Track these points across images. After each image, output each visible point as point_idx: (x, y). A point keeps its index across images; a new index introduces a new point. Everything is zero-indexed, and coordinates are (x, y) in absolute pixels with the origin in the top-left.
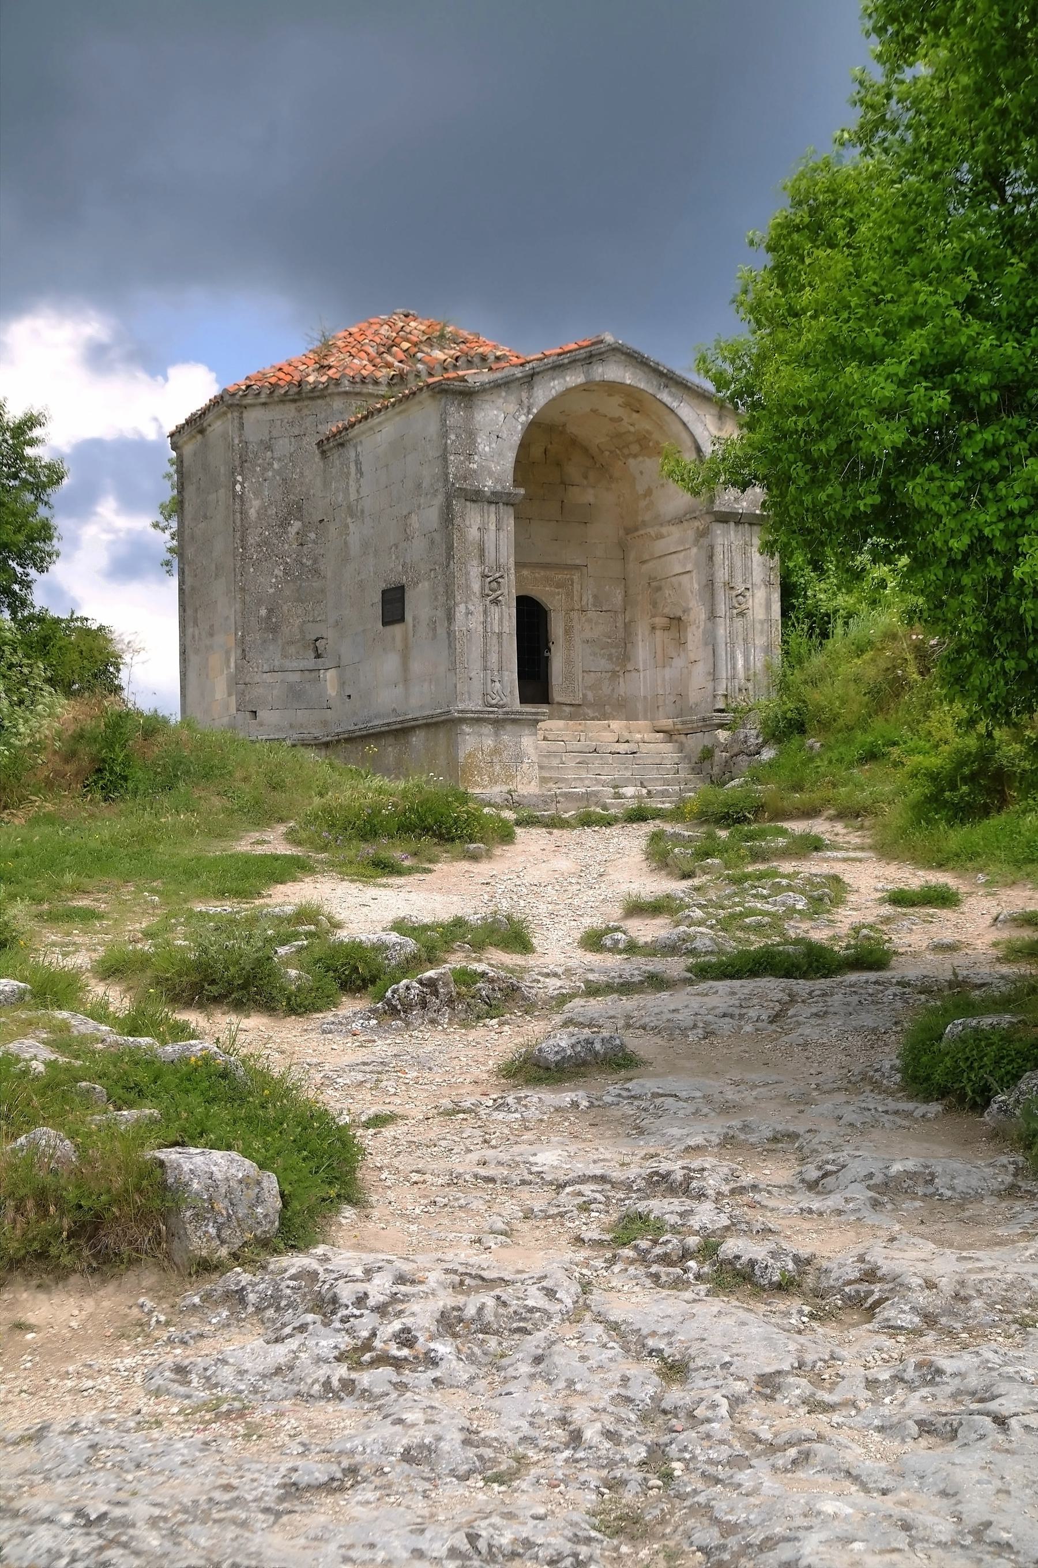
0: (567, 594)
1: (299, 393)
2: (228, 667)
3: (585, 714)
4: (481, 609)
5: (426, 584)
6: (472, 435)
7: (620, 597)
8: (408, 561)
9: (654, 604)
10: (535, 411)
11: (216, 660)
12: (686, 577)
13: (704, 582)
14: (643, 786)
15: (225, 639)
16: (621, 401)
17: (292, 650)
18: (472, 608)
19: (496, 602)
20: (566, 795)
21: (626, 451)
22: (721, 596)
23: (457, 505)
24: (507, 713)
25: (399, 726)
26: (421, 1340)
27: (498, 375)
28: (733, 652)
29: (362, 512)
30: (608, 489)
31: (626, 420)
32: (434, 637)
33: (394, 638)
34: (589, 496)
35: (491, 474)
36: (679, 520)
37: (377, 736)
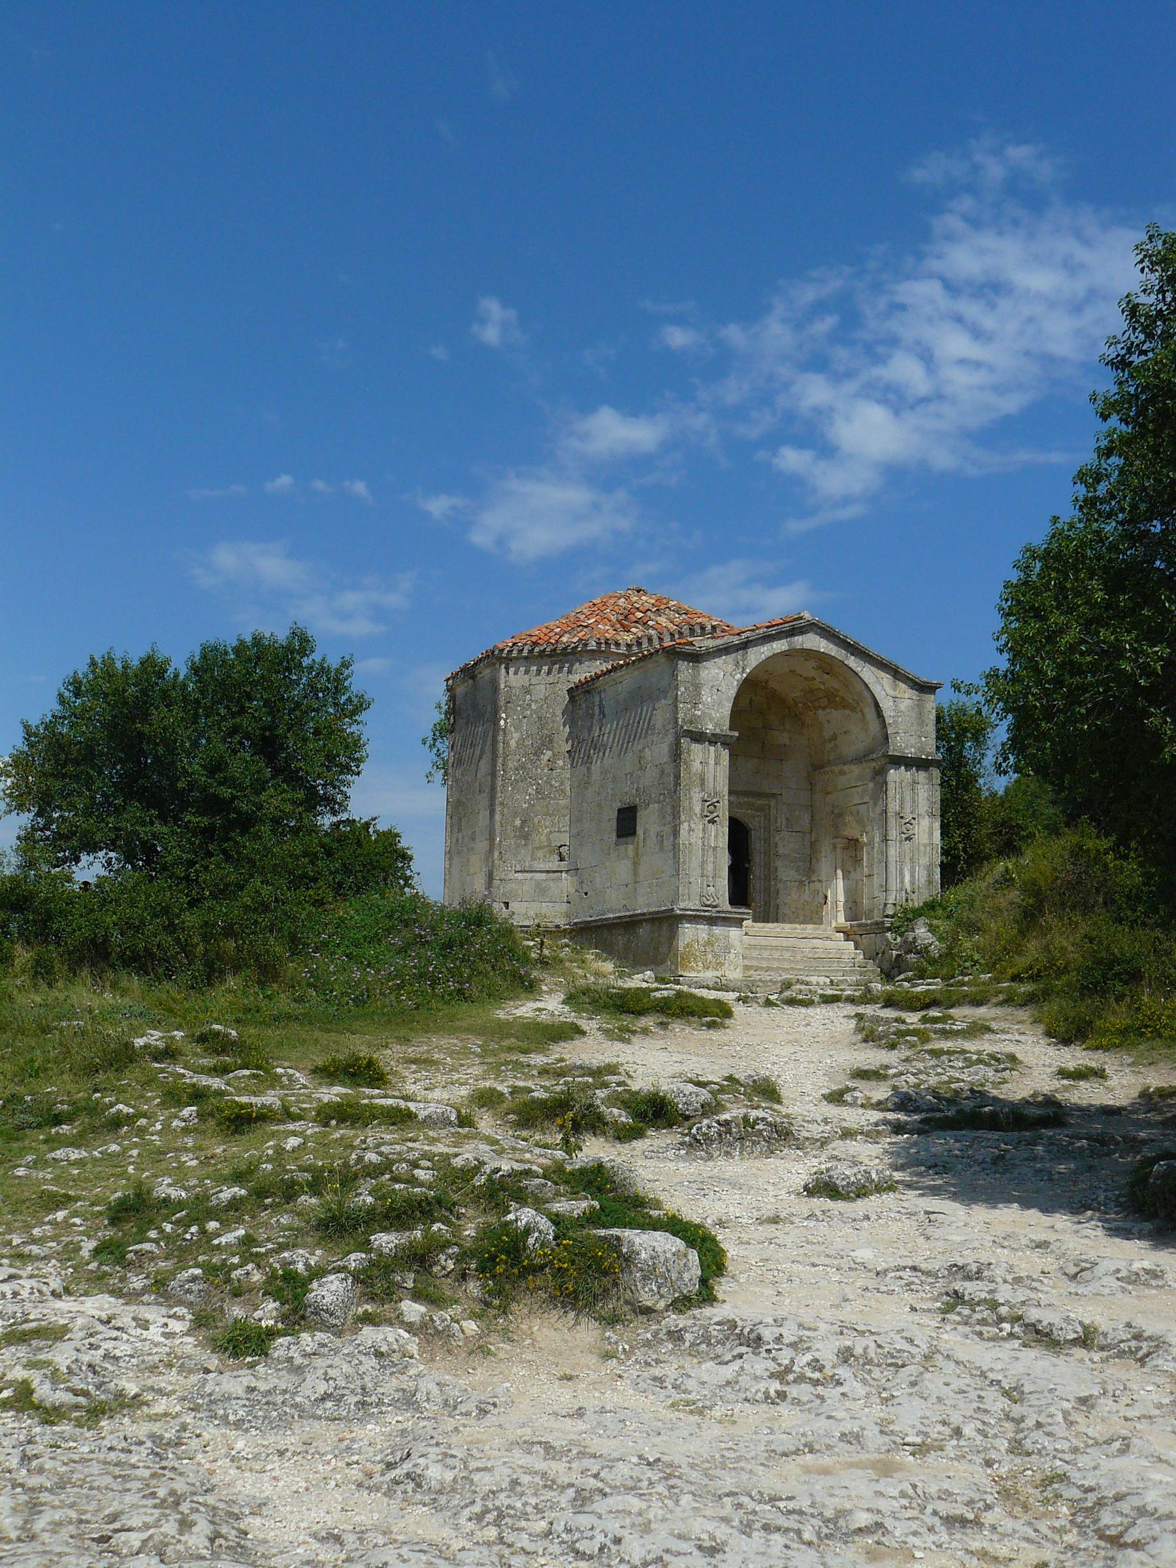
4: (701, 827)
6: (697, 687)
7: (808, 821)
9: (836, 827)
12: (865, 806)
16: (814, 664)
17: (540, 854)
18: (693, 826)
19: (712, 821)
23: (684, 741)
26: (827, 1367)
27: (719, 642)
28: (901, 870)
31: (818, 679)
34: (783, 738)
35: (711, 719)
36: (859, 760)
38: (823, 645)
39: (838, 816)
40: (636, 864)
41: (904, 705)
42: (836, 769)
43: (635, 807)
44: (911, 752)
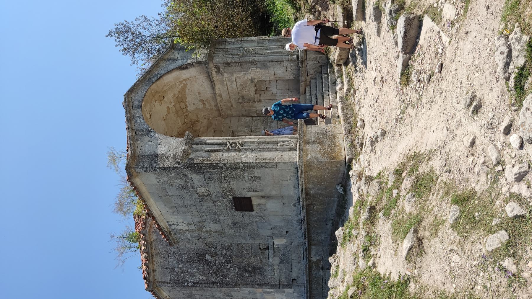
2: (272, 292)
5: (232, 183)
7: (247, 118)
8: (220, 195)
9: (249, 100)
13: (239, 68)
17: (264, 261)
21: (184, 110)
22: (244, 59)
28: (271, 53)
29: (200, 222)
31: (169, 105)
32: (259, 178)
33: (260, 204)
39: (243, 99)
42: (219, 99)
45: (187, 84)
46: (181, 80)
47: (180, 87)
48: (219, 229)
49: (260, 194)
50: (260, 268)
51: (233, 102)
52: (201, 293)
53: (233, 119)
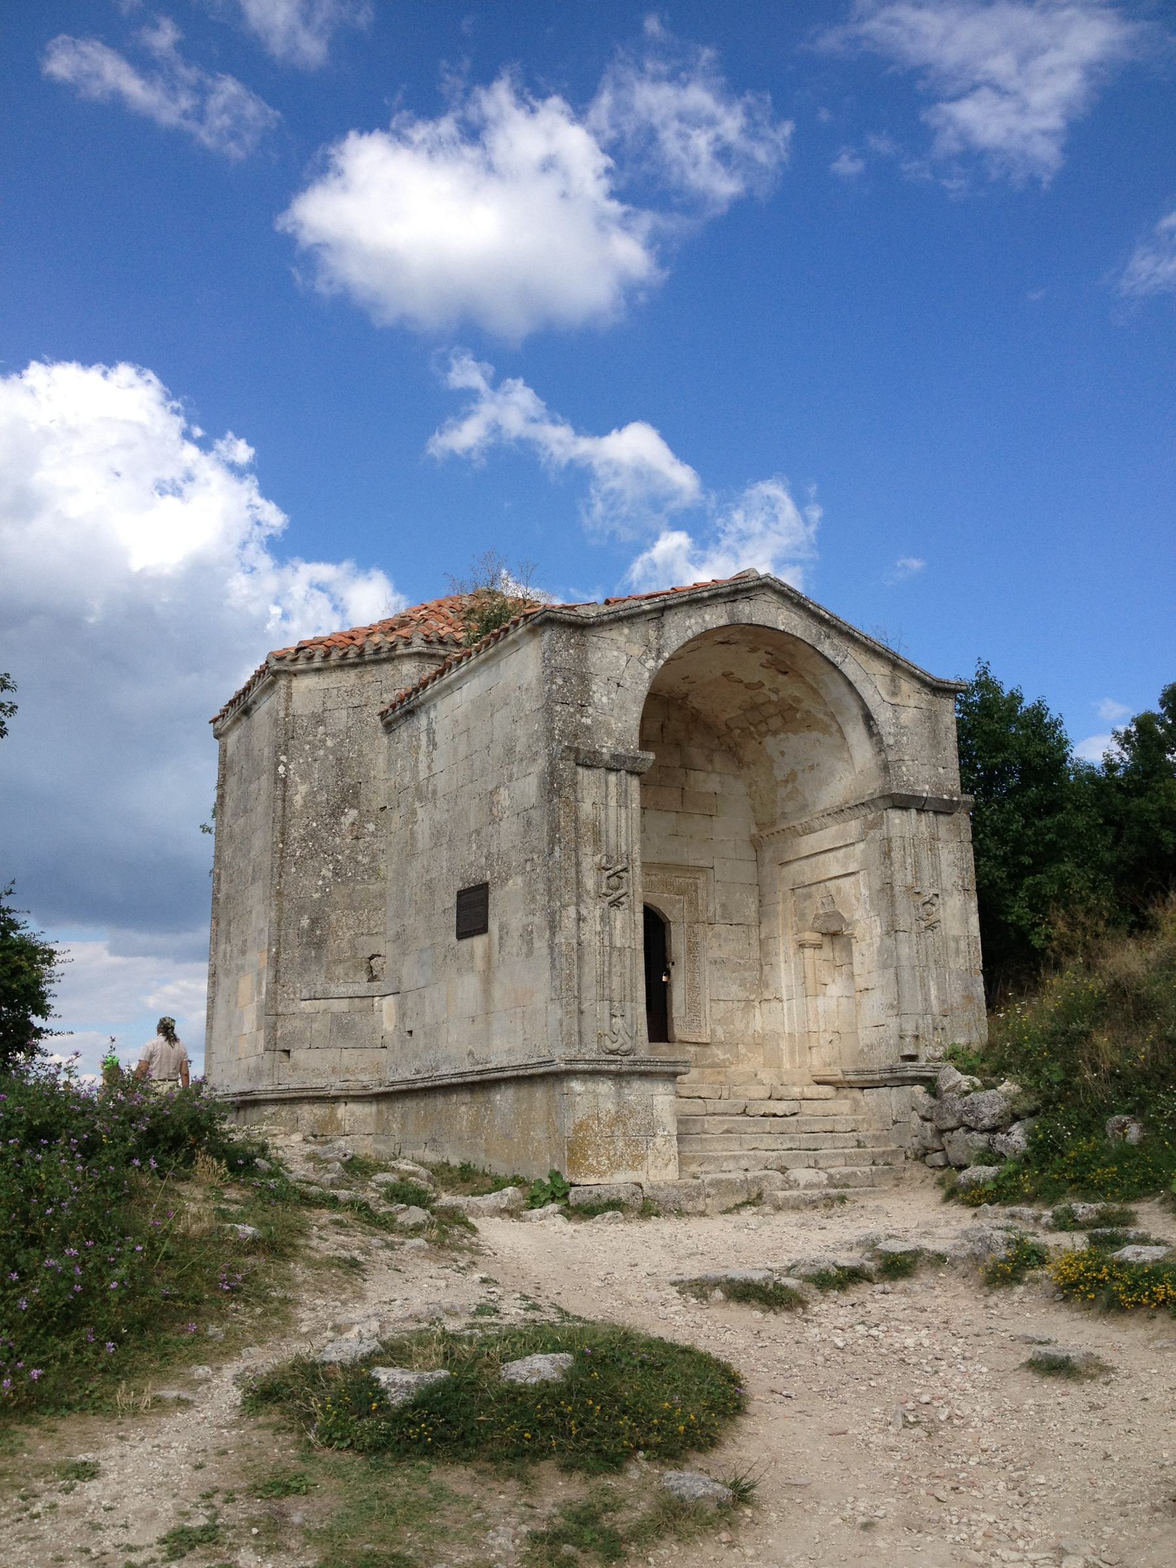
0: (690, 903)
1: (361, 654)
2: (260, 993)
3: (714, 1056)
4: (598, 913)
5: (519, 880)
6: (584, 679)
7: (753, 908)
10: (666, 655)
11: (246, 984)
12: (852, 879)
13: (877, 885)
14: (816, 1166)
15: (258, 958)
17: (339, 970)
18: (584, 912)
19: (616, 903)
20: (716, 1184)
21: (763, 728)
22: (902, 903)
24: (634, 1063)
25: (477, 1078)
29: (434, 792)
30: (736, 777)
31: (767, 686)
35: (609, 733)
37: (447, 1089)
38: (783, 619)
40: (487, 981)
41: (908, 716)
43: (487, 884)
44: (925, 790)
45: (831, 734)
46: (839, 719)
47: (821, 716)
48: (420, 845)
49: (496, 956)
50: (318, 958)
51: (795, 867)
52: (263, 797)
53: (751, 867)
